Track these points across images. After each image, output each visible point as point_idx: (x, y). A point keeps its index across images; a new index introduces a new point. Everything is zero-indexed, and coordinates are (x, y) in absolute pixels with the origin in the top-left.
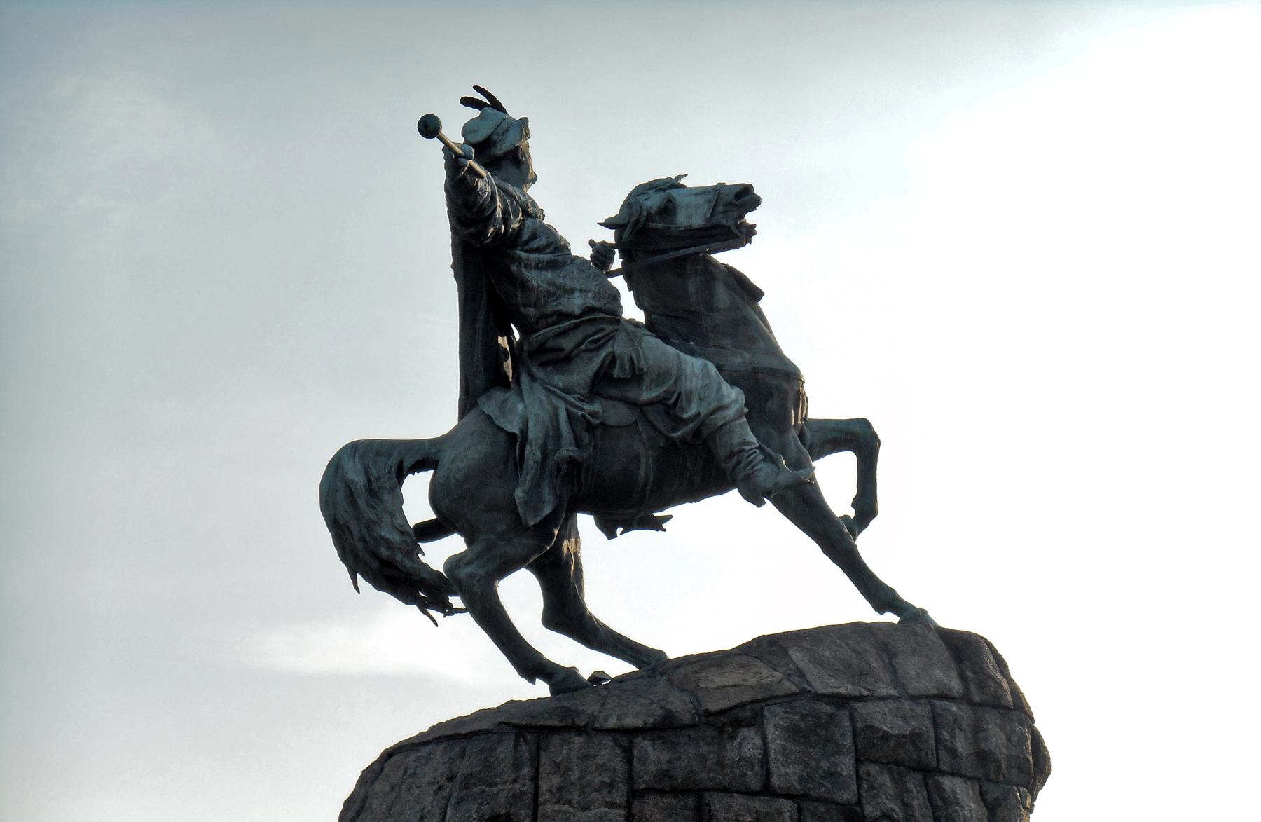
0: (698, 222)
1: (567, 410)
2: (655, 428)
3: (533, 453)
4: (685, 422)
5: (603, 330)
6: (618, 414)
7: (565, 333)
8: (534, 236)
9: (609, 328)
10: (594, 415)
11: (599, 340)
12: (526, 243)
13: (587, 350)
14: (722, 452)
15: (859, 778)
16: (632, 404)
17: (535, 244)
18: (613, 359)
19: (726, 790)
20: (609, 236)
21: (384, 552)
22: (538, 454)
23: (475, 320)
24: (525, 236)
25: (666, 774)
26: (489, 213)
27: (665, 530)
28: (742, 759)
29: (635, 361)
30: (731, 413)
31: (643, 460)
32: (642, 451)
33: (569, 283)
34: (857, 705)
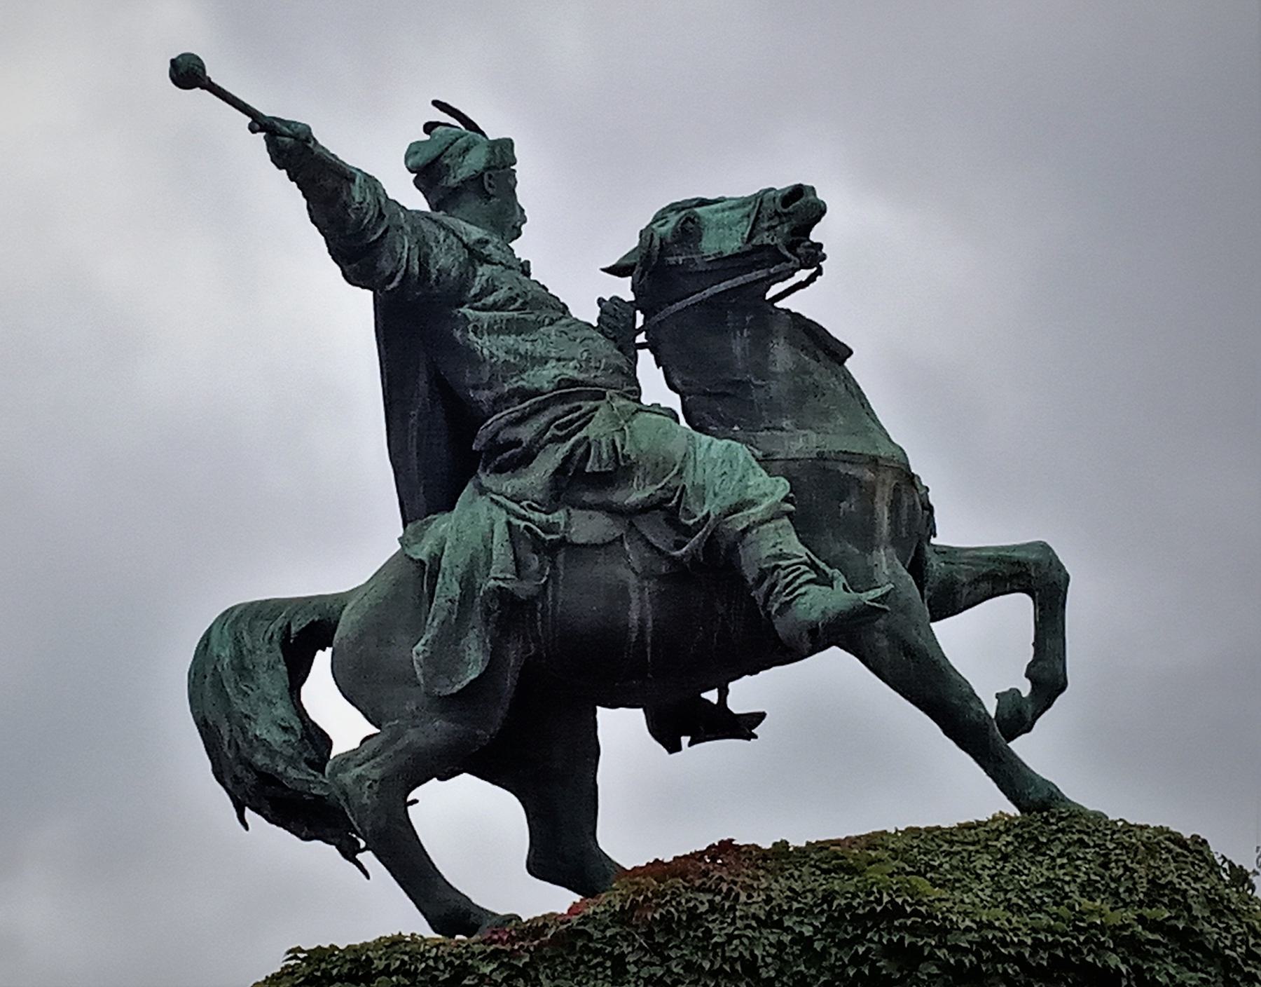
0: (733, 245)
1: (509, 523)
3: (448, 588)
5: (580, 408)
9: (587, 405)
10: (549, 528)
11: (571, 422)
13: (550, 441)
14: (751, 574)
16: (613, 511)
17: (490, 299)
20: (623, 289)
21: (260, 759)
22: (456, 590)
23: (405, 417)
26: (375, 237)
27: (755, 737)
29: (618, 445)
31: (634, 596)
32: (633, 580)
33: (540, 349)
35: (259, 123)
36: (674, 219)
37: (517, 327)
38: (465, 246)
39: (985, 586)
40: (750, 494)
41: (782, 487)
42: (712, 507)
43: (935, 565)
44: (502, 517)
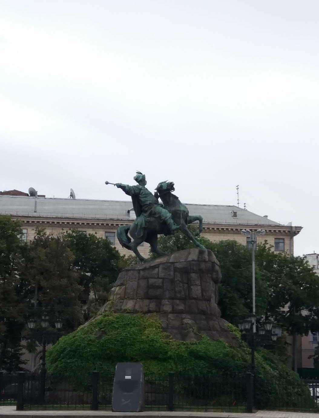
0: (165, 188)
1: (144, 220)
4: (162, 220)
7: (146, 207)
8: (142, 193)
10: (148, 220)
12: (141, 194)
16: (155, 218)
17: (142, 194)
20: (156, 191)
21: (123, 242)
30: (168, 218)
33: (148, 199)
35: (115, 185)
36: (160, 185)
37: (146, 197)
38: (139, 189)
40: (167, 216)
41: (171, 214)
42: (163, 218)
44: (144, 219)
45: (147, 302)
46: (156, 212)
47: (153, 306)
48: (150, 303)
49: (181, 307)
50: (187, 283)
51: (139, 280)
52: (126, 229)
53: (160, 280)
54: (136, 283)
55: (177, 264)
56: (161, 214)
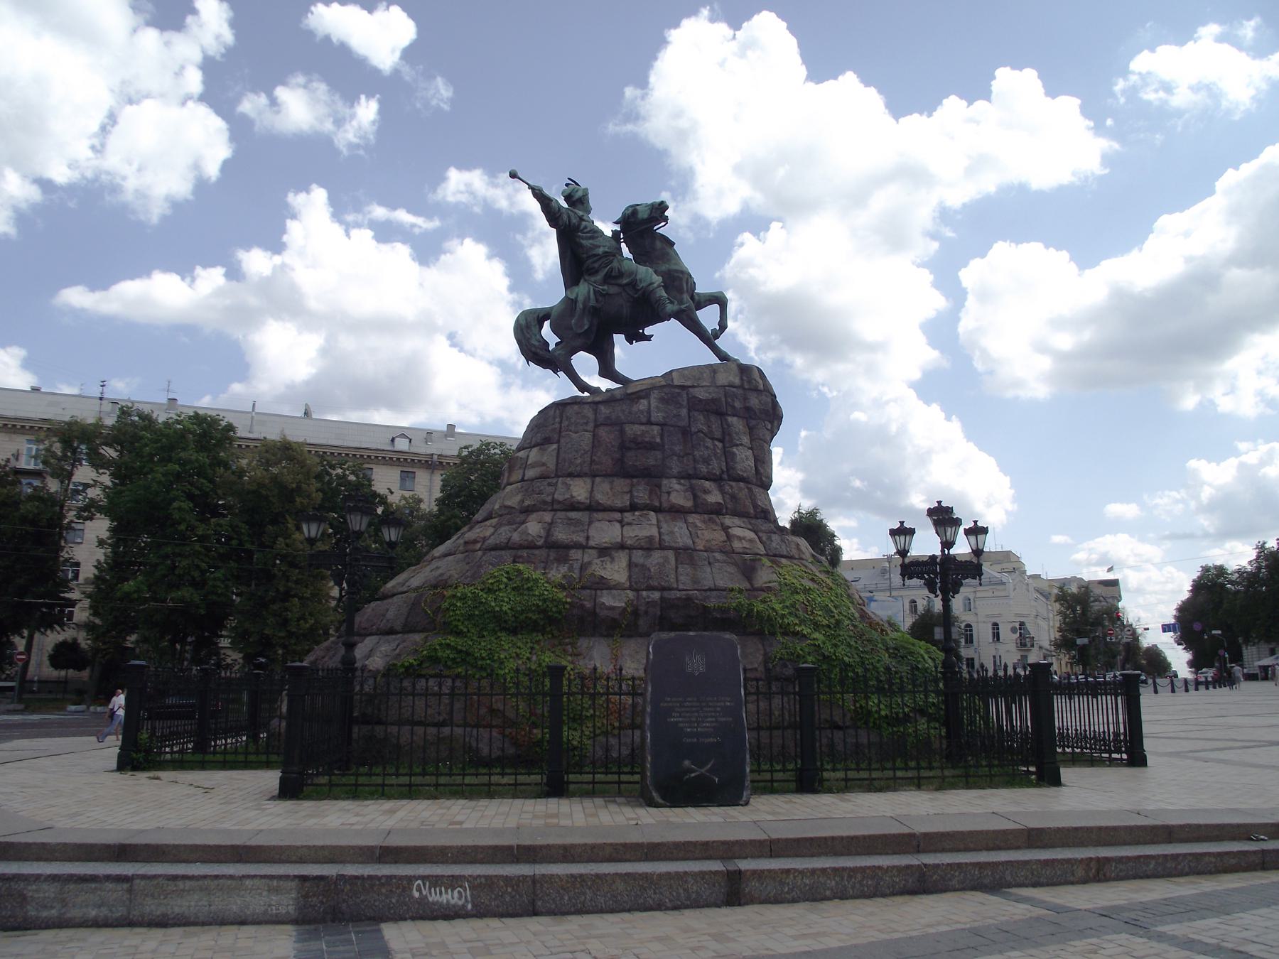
0: (646, 216)
2: (628, 294)
3: (580, 305)
4: (639, 290)
6: (613, 290)
7: (594, 262)
9: (611, 258)
10: (603, 290)
15: (689, 417)
17: (585, 231)
18: (612, 269)
19: (633, 423)
20: (618, 228)
21: (533, 349)
24: (582, 227)
25: (608, 418)
28: (639, 410)
33: (598, 243)
34: (691, 390)
35: (531, 187)
36: (631, 210)
39: (708, 303)
43: (696, 297)
45: (621, 484)
46: (623, 270)
47: (642, 495)
48: (632, 485)
49: (714, 497)
50: (721, 441)
51: (596, 426)
52: (541, 316)
53: (656, 429)
54: (588, 435)
55: (696, 389)
56: (636, 275)
